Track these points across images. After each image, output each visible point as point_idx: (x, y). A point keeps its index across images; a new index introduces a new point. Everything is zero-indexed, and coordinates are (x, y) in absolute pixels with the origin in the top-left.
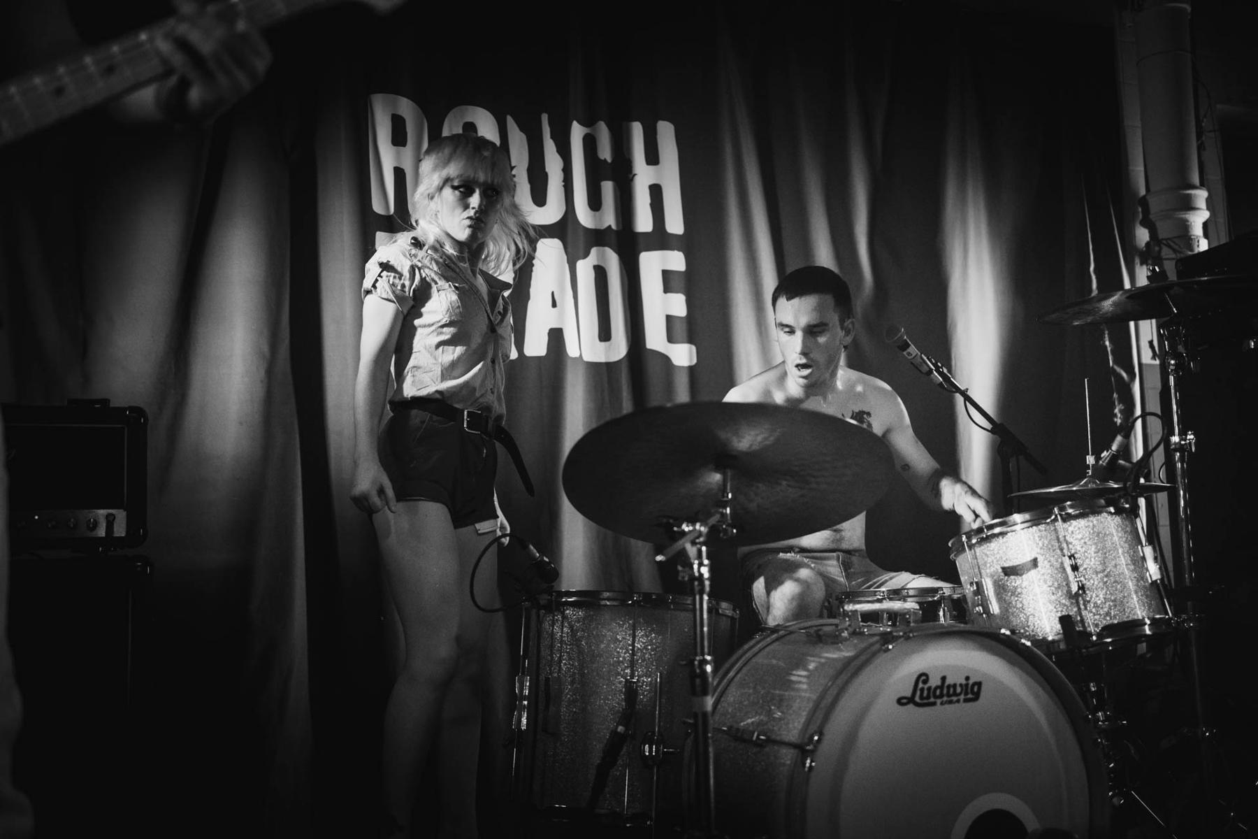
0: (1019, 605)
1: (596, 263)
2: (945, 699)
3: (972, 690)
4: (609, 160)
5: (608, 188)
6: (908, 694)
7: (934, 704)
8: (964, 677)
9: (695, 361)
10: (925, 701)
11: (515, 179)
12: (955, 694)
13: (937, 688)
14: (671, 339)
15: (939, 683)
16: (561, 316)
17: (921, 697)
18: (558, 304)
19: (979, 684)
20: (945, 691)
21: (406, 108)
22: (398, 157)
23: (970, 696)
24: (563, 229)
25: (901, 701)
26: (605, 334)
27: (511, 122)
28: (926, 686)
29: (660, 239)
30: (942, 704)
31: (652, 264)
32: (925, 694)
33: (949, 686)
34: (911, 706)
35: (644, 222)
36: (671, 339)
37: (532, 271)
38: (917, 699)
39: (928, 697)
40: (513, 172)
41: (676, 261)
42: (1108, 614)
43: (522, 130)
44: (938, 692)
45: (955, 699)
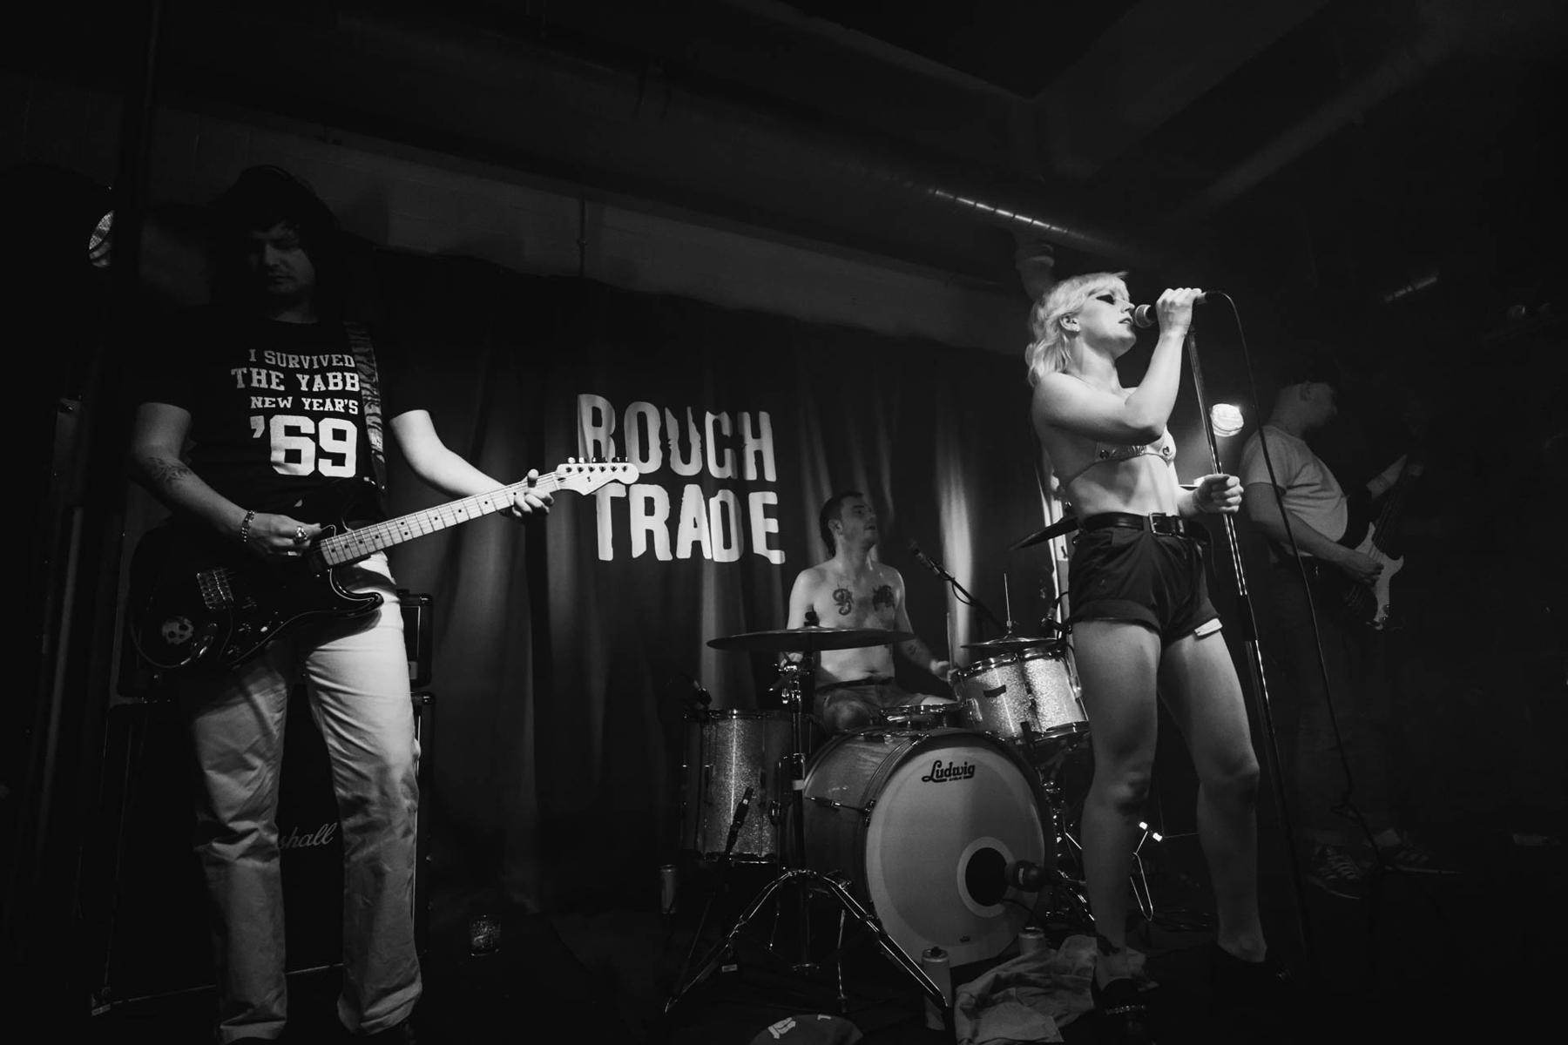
0: (995, 716)
1: (721, 499)
2: (952, 777)
4: (729, 435)
5: (728, 452)
7: (945, 780)
9: (784, 561)
11: (671, 448)
12: (958, 774)
13: (946, 770)
14: (770, 547)
16: (700, 533)
17: (937, 776)
18: (698, 525)
19: (973, 767)
20: (952, 772)
21: (601, 403)
22: (596, 433)
23: (968, 775)
24: (702, 479)
25: (923, 779)
26: (727, 545)
27: (668, 412)
29: (761, 485)
30: (950, 780)
31: (757, 501)
33: (954, 769)
34: (931, 782)
35: (751, 474)
36: (770, 546)
37: (681, 505)
38: (935, 777)
39: (941, 776)
40: (670, 443)
41: (772, 498)
43: (675, 416)
44: (948, 773)
45: (958, 776)
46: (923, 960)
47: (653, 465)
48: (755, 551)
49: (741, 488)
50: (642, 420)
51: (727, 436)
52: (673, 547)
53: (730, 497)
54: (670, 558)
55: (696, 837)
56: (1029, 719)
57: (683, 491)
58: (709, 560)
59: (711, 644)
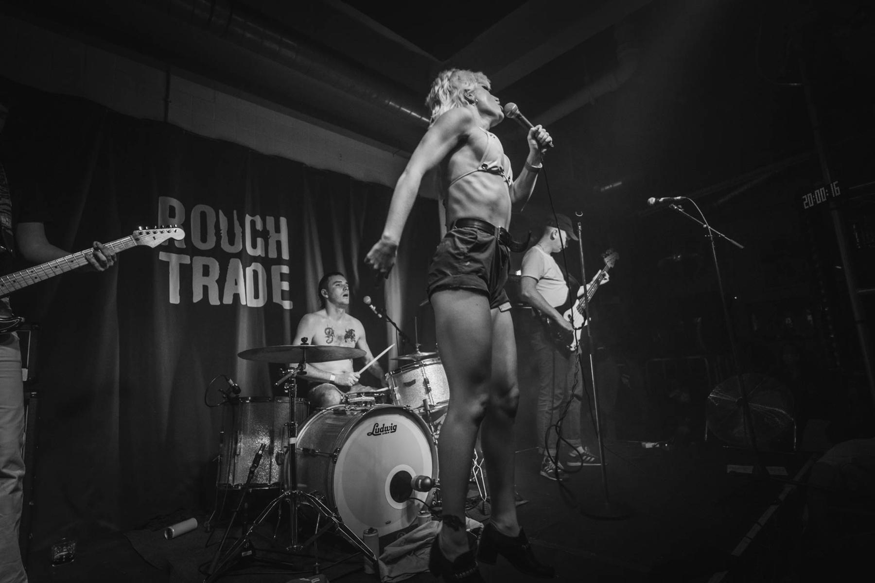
2: (384, 432)
4: (261, 230)
5: (259, 241)
7: (380, 434)
12: (388, 430)
15: (382, 427)
17: (376, 433)
19: (396, 426)
23: (393, 430)
26: (256, 296)
32: (377, 430)
38: (374, 433)
39: (378, 432)
40: (221, 232)
42: (439, 398)
43: (225, 215)
45: (387, 432)
46: (364, 536)
47: (210, 244)
48: (274, 301)
49: (267, 263)
50: (203, 215)
51: (259, 230)
52: (221, 297)
53: (259, 267)
54: (218, 303)
55: (229, 476)
56: (426, 397)
57: (229, 263)
58: (244, 305)
59: (243, 355)
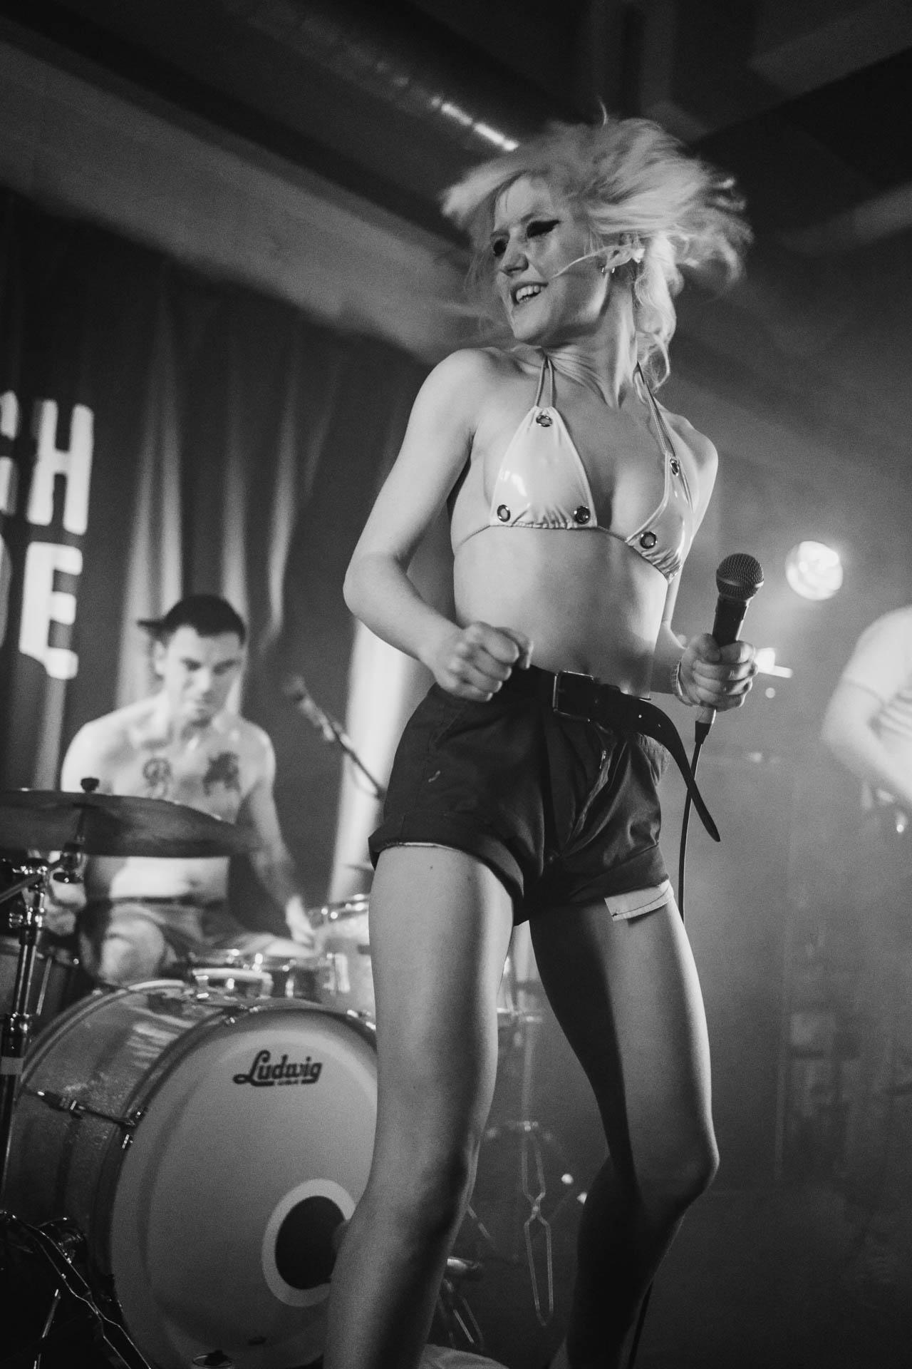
3: (311, 1072)
6: (247, 1072)
7: (271, 1084)
8: (305, 1058)
10: (263, 1080)
12: (295, 1075)
13: (277, 1067)
14: (51, 643)
15: (279, 1062)
17: (260, 1076)
19: (319, 1066)
20: (285, 1071)
23: (309, 1077)
25: (237, 1079)
28: (266, 1064)
29: (55, 533)
30: (280, 1084)
32: (265, 1072)
33: (289, 1067)
34: (248, 1085)
35: (40, 512)
38: (255, 1078)
39: (267, 1077)
44: (277, 1072)
45: (293, 1079)
